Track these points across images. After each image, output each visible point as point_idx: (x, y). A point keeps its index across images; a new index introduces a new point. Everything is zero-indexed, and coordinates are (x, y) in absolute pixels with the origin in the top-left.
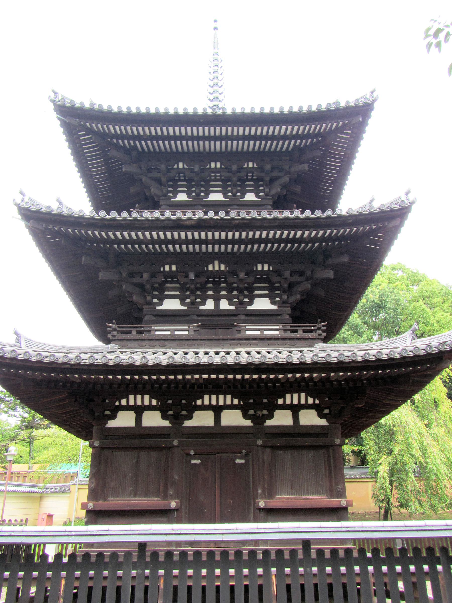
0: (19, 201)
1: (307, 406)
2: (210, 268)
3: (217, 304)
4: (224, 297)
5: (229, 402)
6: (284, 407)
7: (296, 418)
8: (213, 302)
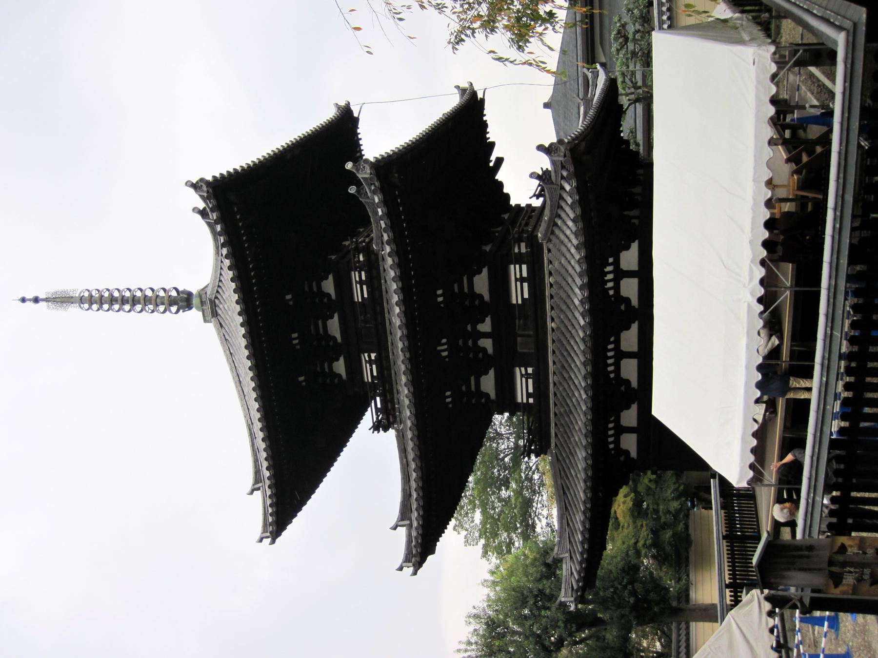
1: (617, 263)
3: (486, 335)
6: (617, 288)
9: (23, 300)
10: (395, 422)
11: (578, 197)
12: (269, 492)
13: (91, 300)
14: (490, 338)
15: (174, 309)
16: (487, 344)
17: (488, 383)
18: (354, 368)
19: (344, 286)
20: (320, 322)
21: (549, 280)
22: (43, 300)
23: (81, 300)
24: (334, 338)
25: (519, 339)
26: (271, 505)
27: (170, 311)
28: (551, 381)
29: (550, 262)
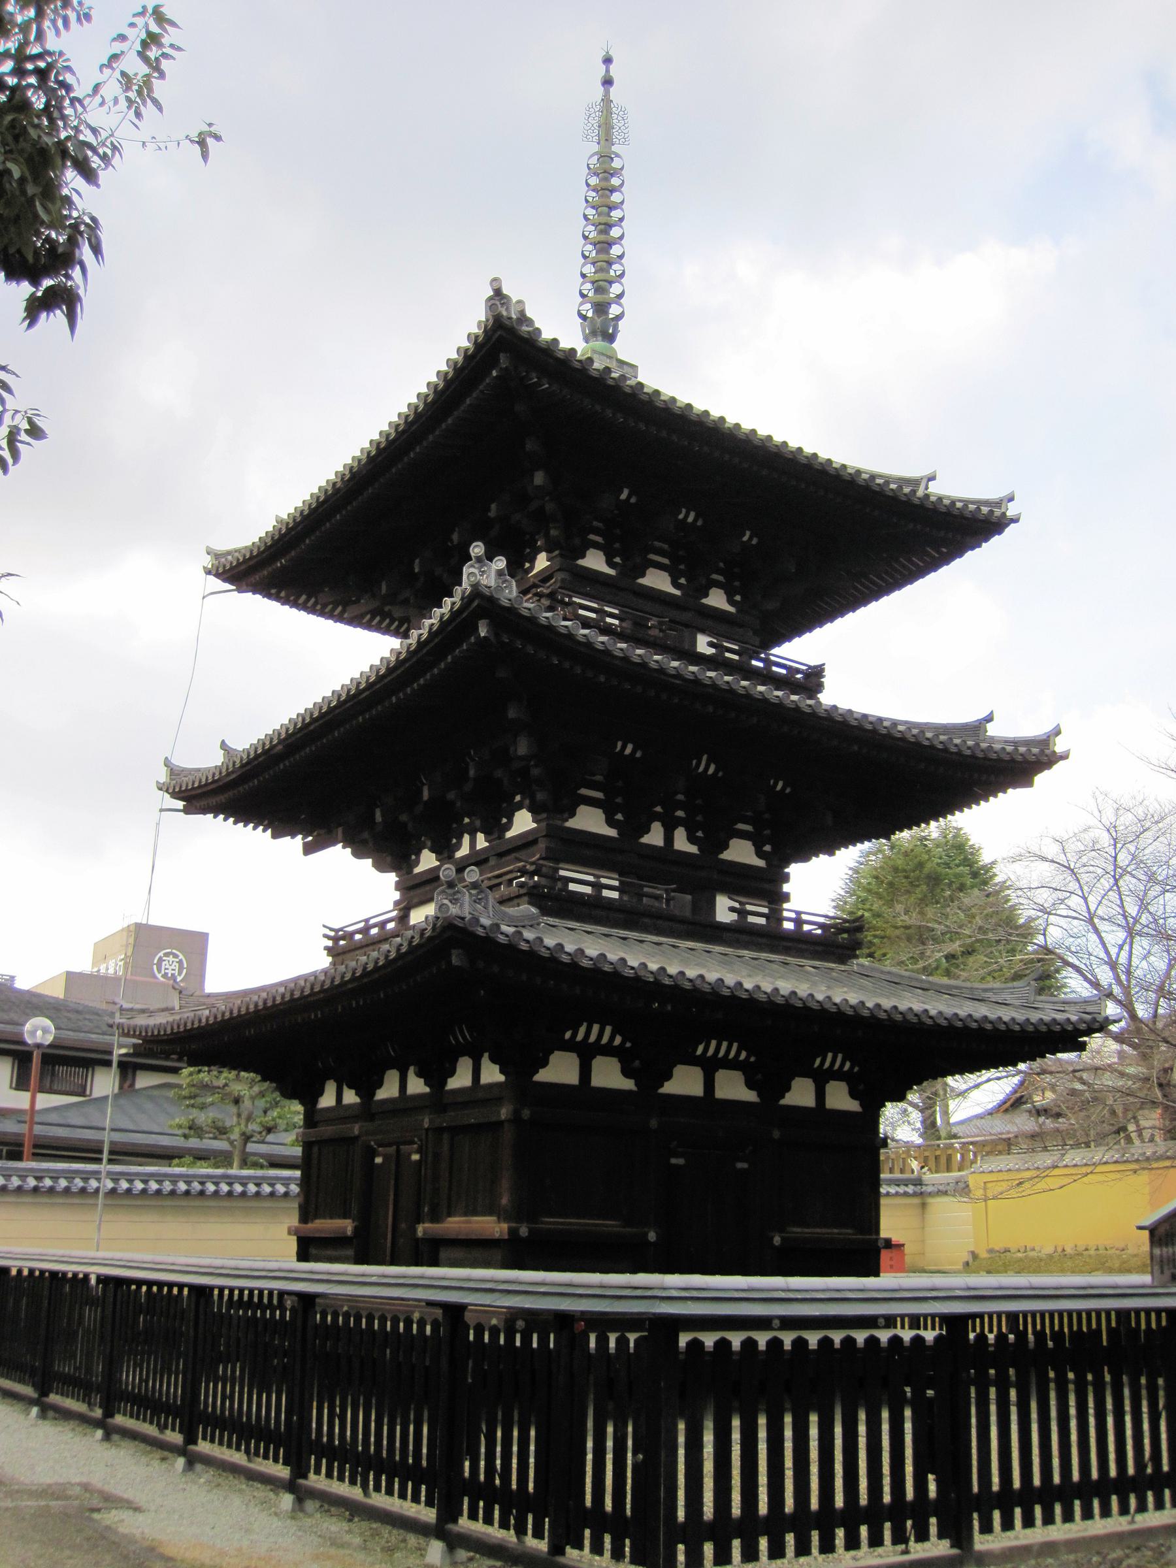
3: (669, 839)
4: (678, 822)
8: (661, 830)
9: (608, 61)
16: (655, 837)
19: (713, 621)
22: (607, 94)
23: (606, 157)
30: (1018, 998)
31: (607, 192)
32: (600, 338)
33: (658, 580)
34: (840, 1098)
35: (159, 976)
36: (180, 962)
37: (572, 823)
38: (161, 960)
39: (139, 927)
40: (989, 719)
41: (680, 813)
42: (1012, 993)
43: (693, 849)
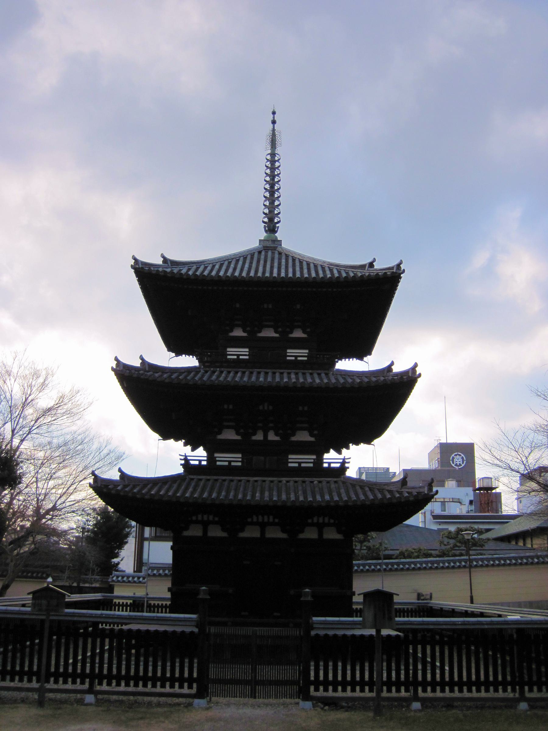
0: (115, 367)
1: (329, 525)
2: (261, 408)
3: (265, 436)
5: (271, 519)
6: (312, 525)
7: (321, 534)
9: (274, 113)
10: (205, 366)
11: (403, 501)
12: (160, 269)
13: (273, 162)
14: (264, 438)
15: (266, 220)
16: (259, 436)
17: (230, 435)
18: (238, 342)
19: (298, 344)
20: (272, 323)
21: (316, 481)
23: (273, 155)
24: (260, 332)
25: (262, 458)
26: (158, 271)
27: (264, 218)
28: (242, 478)
29: (304, 482)
30: (396, 488)
31: (272, 170)
32: (269, 233)
33: (269, 333)
34: (331, 534)
35: (453, 465)
36: (462, 458)
37: (220, 437)
38: (453, 458)
39: (441, 444)
40: (392, 364)
41: (271, 425)
42: (394, 486)
43: (277, 438)
